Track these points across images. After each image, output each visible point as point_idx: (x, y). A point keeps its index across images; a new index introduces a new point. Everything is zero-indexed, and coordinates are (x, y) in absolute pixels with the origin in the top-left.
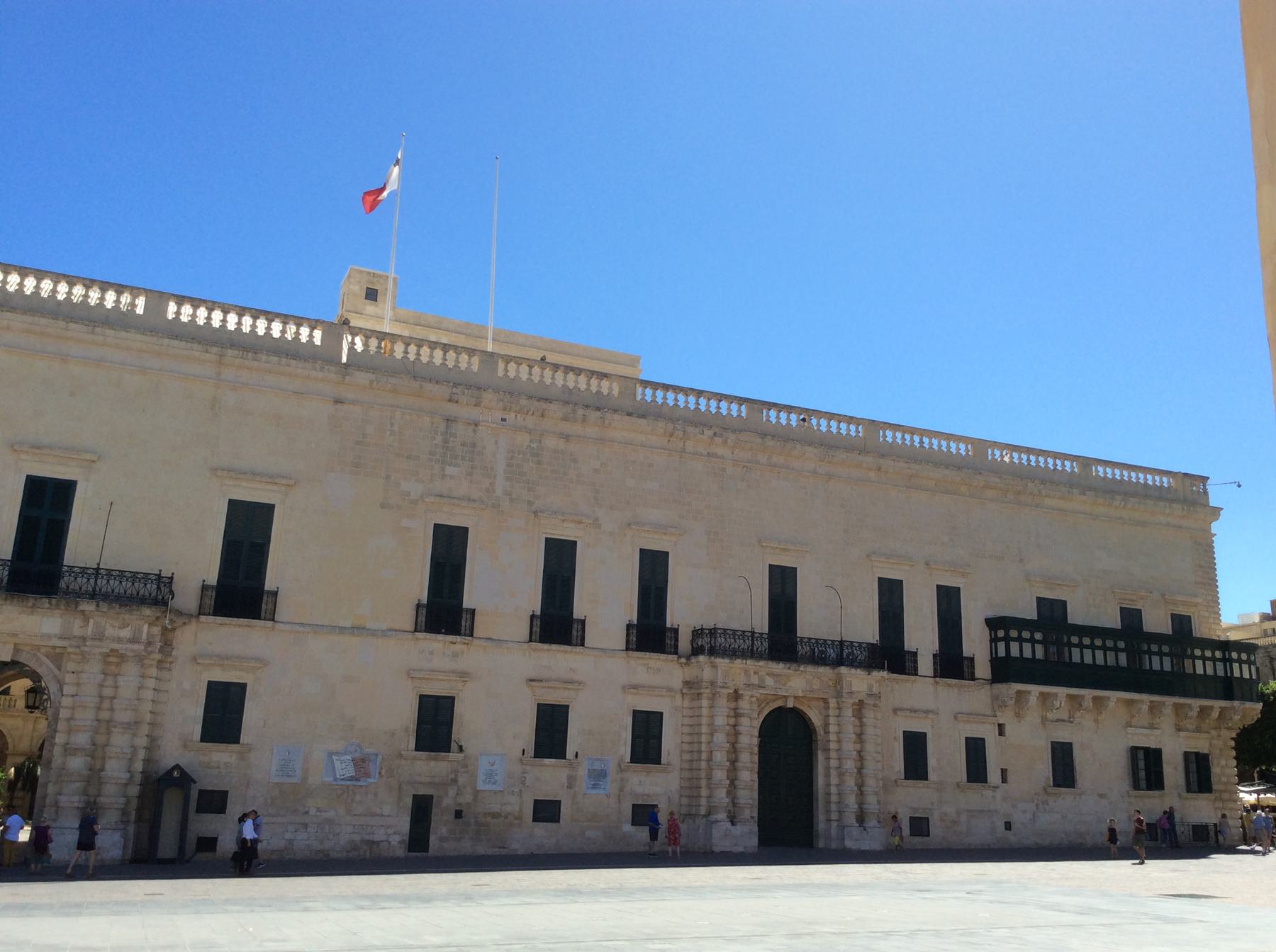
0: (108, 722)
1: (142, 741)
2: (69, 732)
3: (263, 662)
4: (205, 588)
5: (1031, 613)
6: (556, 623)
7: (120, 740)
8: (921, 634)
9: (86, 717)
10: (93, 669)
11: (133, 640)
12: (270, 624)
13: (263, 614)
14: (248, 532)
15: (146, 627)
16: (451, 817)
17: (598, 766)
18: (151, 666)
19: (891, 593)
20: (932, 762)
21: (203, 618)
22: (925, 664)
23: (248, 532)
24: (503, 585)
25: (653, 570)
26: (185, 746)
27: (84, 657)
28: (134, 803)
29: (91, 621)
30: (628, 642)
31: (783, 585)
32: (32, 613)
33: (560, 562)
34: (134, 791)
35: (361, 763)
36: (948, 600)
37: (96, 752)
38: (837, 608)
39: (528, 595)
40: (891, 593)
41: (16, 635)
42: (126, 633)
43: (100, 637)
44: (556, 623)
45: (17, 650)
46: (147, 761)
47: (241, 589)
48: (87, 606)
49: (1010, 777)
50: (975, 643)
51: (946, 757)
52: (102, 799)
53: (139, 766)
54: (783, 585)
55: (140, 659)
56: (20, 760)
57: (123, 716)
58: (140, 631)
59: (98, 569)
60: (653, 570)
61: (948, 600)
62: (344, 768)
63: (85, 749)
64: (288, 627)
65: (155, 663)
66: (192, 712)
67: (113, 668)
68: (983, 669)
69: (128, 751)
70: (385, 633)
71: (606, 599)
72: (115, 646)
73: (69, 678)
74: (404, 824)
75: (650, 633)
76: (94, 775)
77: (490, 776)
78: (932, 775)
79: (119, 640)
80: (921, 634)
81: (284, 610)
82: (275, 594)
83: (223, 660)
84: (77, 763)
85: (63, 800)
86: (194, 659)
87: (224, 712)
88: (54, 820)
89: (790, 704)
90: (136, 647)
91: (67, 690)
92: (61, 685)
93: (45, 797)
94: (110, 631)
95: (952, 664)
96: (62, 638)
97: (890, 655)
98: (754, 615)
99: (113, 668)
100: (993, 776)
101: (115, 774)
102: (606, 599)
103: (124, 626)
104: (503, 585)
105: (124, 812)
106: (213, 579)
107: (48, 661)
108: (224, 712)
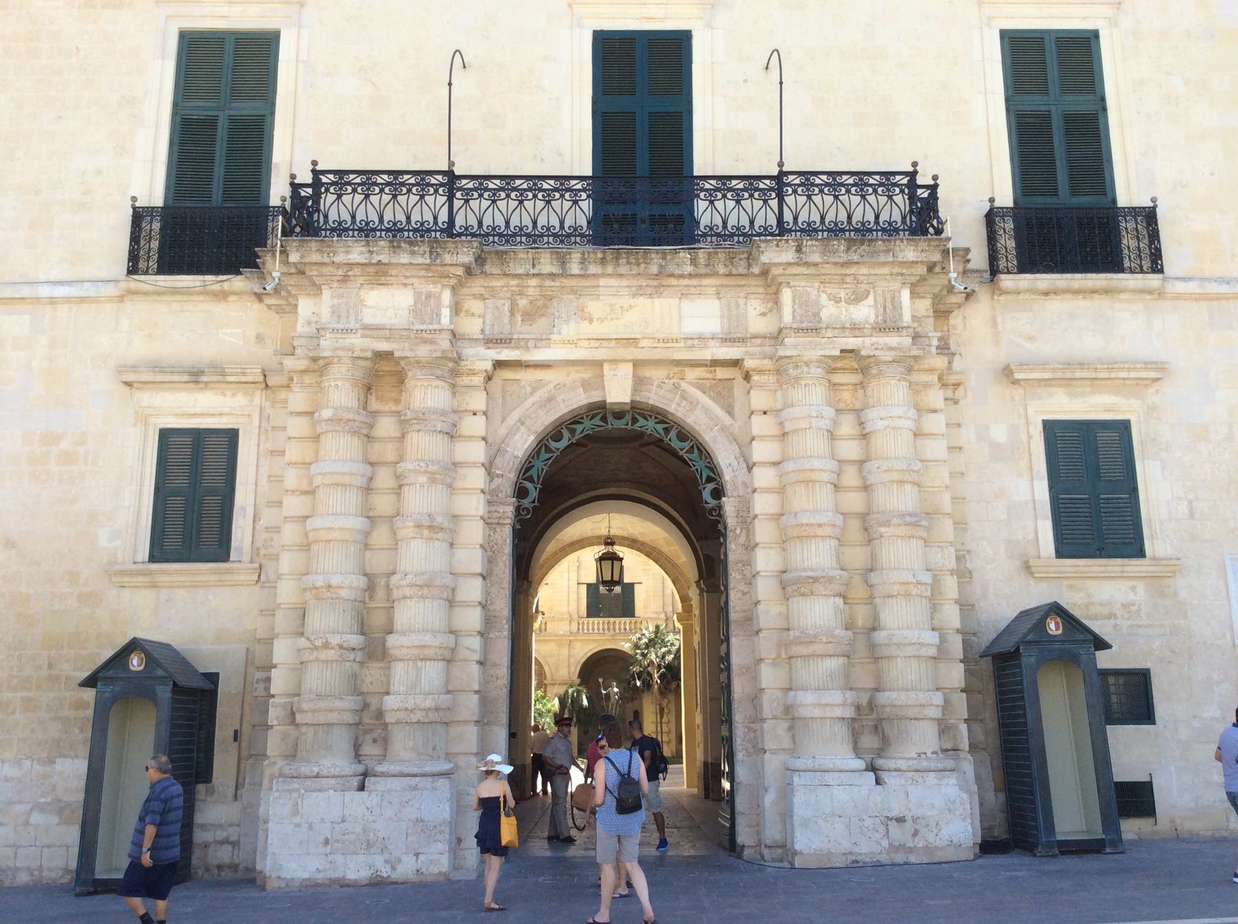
0: (864, 517)
1: (945, 559)
2: (784, 542)
3: (1155, 373)
7: (902, 556)
9: (816, 505)
10: (811, 400)
11: (885, 327)
12: (1154, 280)
13: (1127, 263)
14: (1054, 87)
15: (905, 294)
18: (927, 386)
21: (1007, 281)
23: (1054, 87)
26: (1027, 568)
27: (782, 370)
28: (961, 704)
29: (786, 295)
32: (658, 292)
34: (955, 674)
37: (861, 587)
41: (632, 342)
42: (865, 312)
43: (812, 327)
45: (639, 383)
46: (966, 607)
47: (1069, 216)
48: (776, 254)
52: (883, 698)
53: (951, 617)
55: (908, 364)
56: (562, 690)
57: (902, 500)
58: (897, 307)
59: (782, 174)
63: (830, 580)
64: (1192, 287)
65: (934, 378)
66: (1022, 496)
67: (847, 396)
69: (927, 578)
72: (851, 342)
73: (760, 425)
76: (865, 642)
79: (855, 329)
82: (1149, 216)
83: (1070, 374)
84: (819, 612)
85: (807, 702)
86: (1007, 373)
87: (1094, 491)
88: (793, 752)
90: (893, 340)
91: (762, 451)
92: (744, 445)
93: (755, 698)
94: (829, 311)
96: (728, 340)
99: (847, 396)
101: (913, 636)
103: (857, 299)
105: (945, 729)
107: (704, 399)
108: (1094, 491)
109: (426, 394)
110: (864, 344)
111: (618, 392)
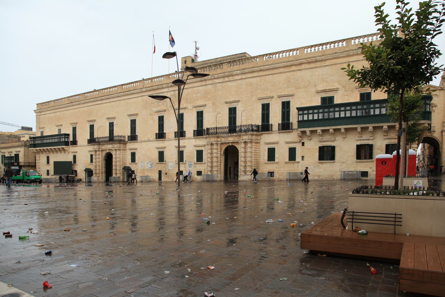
4: (156, 134)
5: (358, 99)
6: (180, 134)
8: (275, 118)
16: (165, 174)
17: (190, 163)
19: (266, 108)
20: (276, 156)
22: (275, 127)
24: (171, 127)
25: (200, 115)
30: (279, 129)
31: (232, 112)
33: (180, 119)
35: (151, 165)
36: (286, 106)
38: (249, 116)
39: (175, 128)
40: (266, 108)
44: (180, 134)
49: (305, 158)
50: (294, 118)
51: (282, 154)
54: (232, 112)
55: (119, 149)
60: (200, 115)
61: (286, 106)
62: (149, 166)
66: (129, 157)
68: (295, 126)
70: (149, 141)
71: (190, 125)
74: (158, 176)
75: (200, 132)
77: (171, 166)
78: (276, 160)
80: (275, 118)
81: (139, 139)
89: (230, 144)
95: (285, 126)
97: (265, 127)
98: (225, 123)
100: (298, 158)
102: (190, 125)
104: (171, 127)
106: (280, 122)
109: (98, 153)
110: (116, 148)
111: (108, 152)
